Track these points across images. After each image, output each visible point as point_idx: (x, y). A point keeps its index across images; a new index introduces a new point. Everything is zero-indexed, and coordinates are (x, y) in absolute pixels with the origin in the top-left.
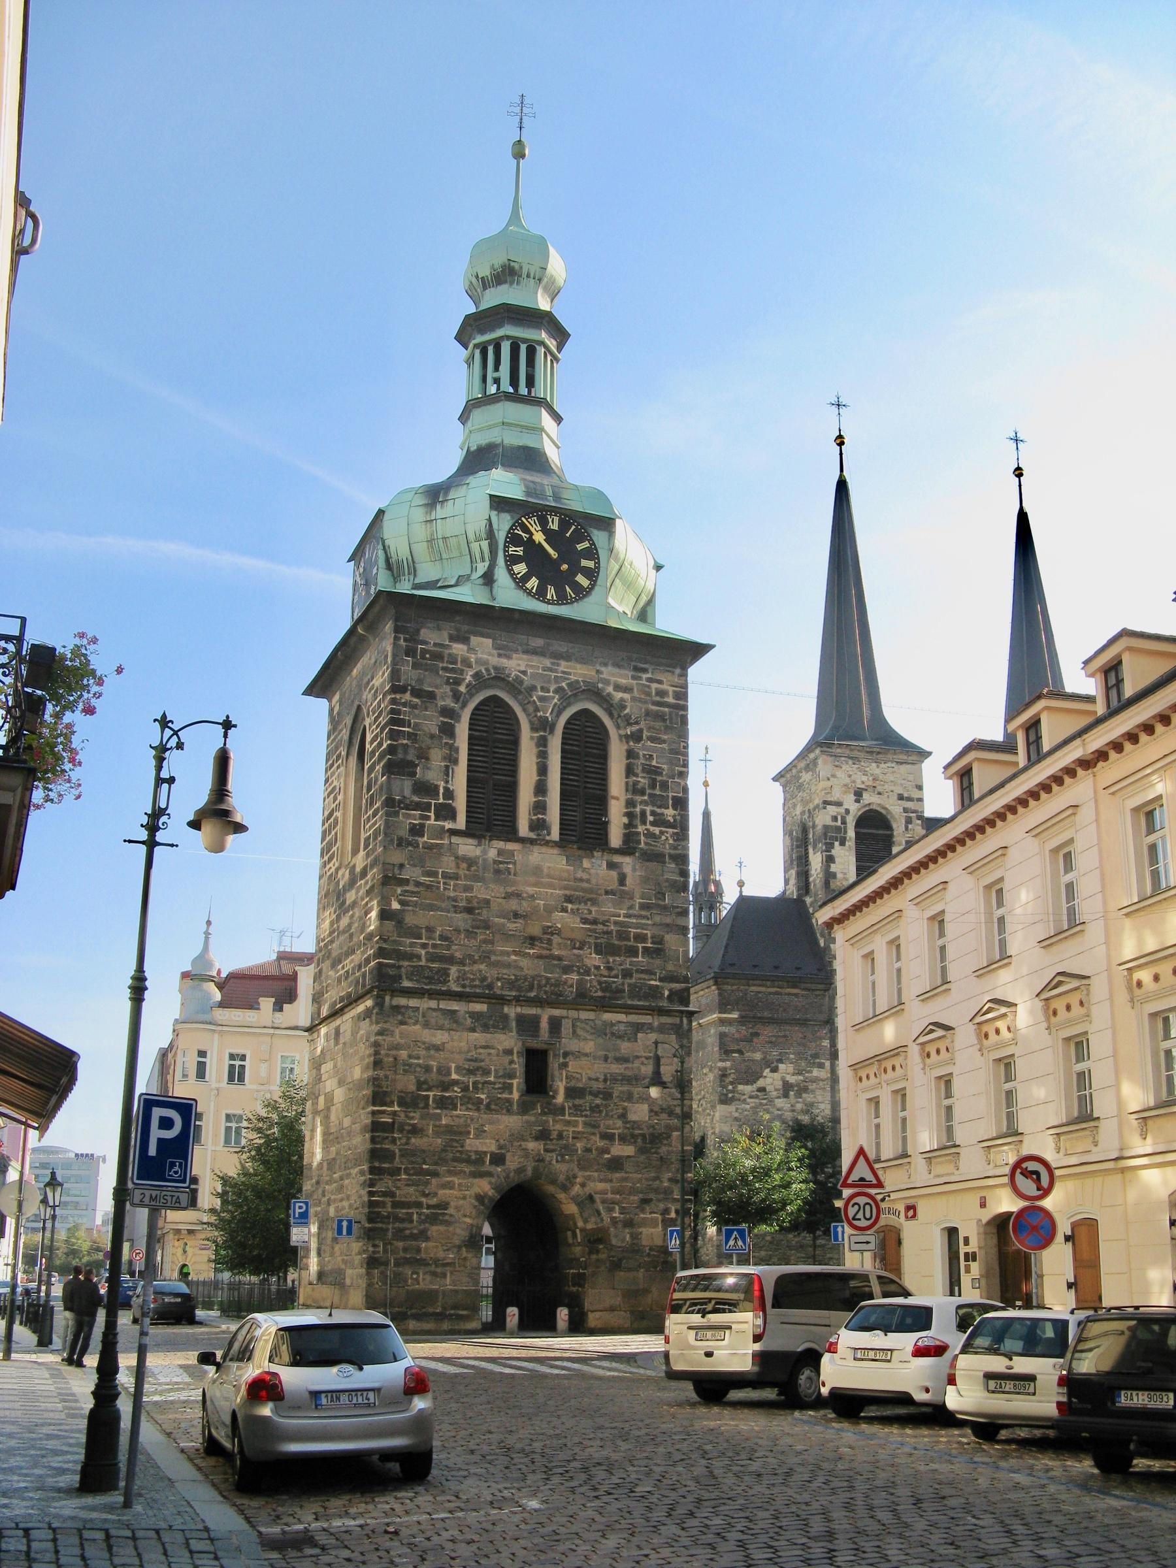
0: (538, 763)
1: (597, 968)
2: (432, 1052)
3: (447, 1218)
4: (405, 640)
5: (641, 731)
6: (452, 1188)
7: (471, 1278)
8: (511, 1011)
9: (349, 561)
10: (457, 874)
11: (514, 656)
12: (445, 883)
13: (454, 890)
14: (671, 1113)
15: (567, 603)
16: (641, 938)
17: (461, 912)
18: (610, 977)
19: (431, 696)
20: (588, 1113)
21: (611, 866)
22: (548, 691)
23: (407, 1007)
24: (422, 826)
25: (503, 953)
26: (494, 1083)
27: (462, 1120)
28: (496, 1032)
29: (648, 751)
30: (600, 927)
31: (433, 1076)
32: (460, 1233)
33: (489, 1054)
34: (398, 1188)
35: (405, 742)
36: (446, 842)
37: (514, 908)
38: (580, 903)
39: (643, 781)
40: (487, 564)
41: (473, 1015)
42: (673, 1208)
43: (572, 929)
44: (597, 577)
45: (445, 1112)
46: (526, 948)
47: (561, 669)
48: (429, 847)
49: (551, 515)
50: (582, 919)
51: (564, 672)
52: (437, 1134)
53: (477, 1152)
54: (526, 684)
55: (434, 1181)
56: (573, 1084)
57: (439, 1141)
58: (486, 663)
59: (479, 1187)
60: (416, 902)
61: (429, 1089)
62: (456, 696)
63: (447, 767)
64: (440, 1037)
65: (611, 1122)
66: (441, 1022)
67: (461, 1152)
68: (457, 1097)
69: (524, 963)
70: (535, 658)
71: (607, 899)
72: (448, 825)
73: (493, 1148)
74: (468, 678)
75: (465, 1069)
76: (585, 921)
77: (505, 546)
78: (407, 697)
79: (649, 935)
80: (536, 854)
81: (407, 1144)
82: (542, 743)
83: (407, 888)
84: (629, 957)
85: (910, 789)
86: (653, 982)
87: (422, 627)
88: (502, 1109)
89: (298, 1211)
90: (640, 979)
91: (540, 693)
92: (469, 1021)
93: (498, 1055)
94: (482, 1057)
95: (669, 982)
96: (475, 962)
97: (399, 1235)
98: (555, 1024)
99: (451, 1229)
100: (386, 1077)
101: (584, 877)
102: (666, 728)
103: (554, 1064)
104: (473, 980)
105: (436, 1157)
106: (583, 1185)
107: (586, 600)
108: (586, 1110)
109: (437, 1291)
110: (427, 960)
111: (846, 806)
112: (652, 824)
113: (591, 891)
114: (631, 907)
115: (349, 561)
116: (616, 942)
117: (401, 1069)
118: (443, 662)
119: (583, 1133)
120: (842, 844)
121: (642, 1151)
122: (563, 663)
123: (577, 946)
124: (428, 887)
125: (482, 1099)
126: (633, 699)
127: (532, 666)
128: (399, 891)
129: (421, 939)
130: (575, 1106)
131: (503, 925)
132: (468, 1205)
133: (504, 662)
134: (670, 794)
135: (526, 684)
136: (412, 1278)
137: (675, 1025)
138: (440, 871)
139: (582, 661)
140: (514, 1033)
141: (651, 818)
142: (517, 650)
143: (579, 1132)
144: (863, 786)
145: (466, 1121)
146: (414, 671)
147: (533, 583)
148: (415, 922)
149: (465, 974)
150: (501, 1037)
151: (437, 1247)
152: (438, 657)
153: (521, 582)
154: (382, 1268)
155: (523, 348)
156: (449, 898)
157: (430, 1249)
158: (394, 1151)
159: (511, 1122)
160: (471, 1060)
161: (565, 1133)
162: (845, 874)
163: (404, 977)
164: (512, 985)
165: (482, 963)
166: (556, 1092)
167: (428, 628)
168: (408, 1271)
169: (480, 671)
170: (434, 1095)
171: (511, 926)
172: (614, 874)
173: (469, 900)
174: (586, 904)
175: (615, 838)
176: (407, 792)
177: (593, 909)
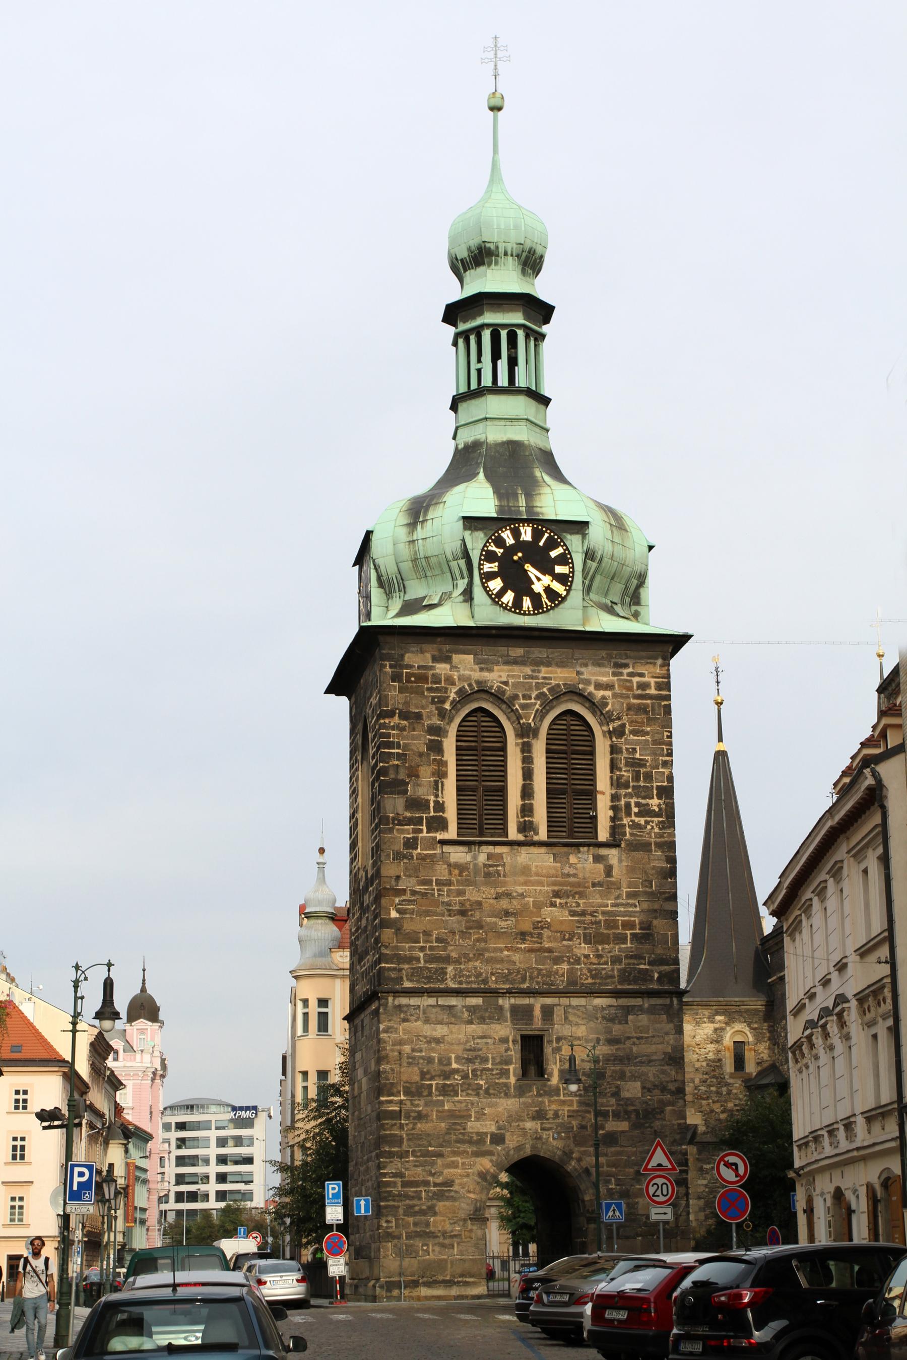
0: (523, 768)
1: (587, 956)
2: (433, 1045)
3: (452, 1194)
4: (391, 666)
5: (623, 726)
6: (457, 1167)
7: (477, 1248)
8: (505, 1003)
9: (354, 565)
10: (450, 880)
11: (496, 668)
12: (438, 890)
13: (448, 896)
14: (664, 1089)
15: (543, 612)
16: (631, 925)
18: (599, 964)
19: (418, 716)
21: (597, 859)
22: (530, 698)
23: (408, 1006)
24: (415, 839)
25: (496, 950)
26: (492, 1070)
27: (464, 1104)
28: (492, 1023)
29: (631, 745)
30: (589, 918)
31: (435, 1067)
32: (464, 1207)
33: (487, 1043)
34: (407, 1169)
35: (396, 762)
36: (438, 851)
37: (504, 907)
38: (568, 897)
39: (626, 774)
40: (466, 581)
43: (562, 922)
44: (572, 582)
45: (447, 1098)
46: (517, 942)
49: (524, 526)
50: (570, 911)
51: (544, 678)
52: (440, 1118)
53: (478, 1134)
54: (508, 694)
55: (439, 1161)
57: (443, 1125)
58: (469, 678)
59: (481, 1165)
60: (413, 909)
61: (432, 1079)
62: (442, 714)
63: (436, 782)
64: (440, 1031)
65: (605, 1100)
66: (440, 1017)
67: (463, 1134)
68: (458, 1084)
69: (516, 957)
70: (515, 668)
72: (440, 836)
73: (493, 1129)
74: (452, 696)
75: (464, 1058)
76: (573, 913)
77: (480, 564)
78: (396, 719)
79: (637, 922)
80: (523, 855)
81: (413, 1129)
82: (526, 749)
83: (404, 898)
84: (617, 944)
86: (642, 967)
87: (406, 652)
88: (501, 1093)
89: (331, 1192)
90: (629, 964)
91: (522, 701)
92: (466, 1014)
93: (494, 1044)
94: (479, 1046)
95: (658, 966)
96: (470, 960)
97: (409, 1211)
98: (548, 1012)
99: (457, 1204)
100: (392, 1070)
101: (571, 873)
102: (649, 719)
103: (548, 1050)
104: (469, 976)
105: (441, 1140)
106: (579, 1160)
107: (561, 606)
109: (446, 1261)
110: (426, 962)
112: (637, 815)
113: (579, 885)
115: (354, 565)
116: (605, 931)
117: (405, 1061)
118: (428, 683)
119: (578, 1111)
121: (635, 1126)
122: (543, 669)
123: (566, 937)
124: (424, 895)
125: (482, 1085)
126: (615, 696)
127: (513, 676)
128: (397, 900)
129: (420, 943)
131: (496, 923)
132: (471, 1182)
133: (486, 675)
134: (655, 785)
135: (508, 694)
136: (423, 1250)
137: (665, 1005)
138: (434, 879)
139: (562, 664)
140: (509, 1023)
141: (636, 810)
142: (499, 663)
143: (573, 1111)
145: (467, 1106)
146: (401, 695)
147: (509, 597)
149: (461, 971)
151: (444, 1221)
152: (423, 678)
153: (496, 598)
154: (396, 1241)
155: (504, 334)
156: (443, 903)
157: (437, 1223)
158: (401, 1137)
159: (508, 1105)
160: (470, 1050)
161: (560, 1113)
163: (405, 979)
164: (505, 978)
165: (476, 961)
166: (551, 1075)
167: (413, 652)
168: (418, 1243)
169: (464, 687)
170: (437, 1084)
171: (503, 924)
172: (600, 867)
173: (462, 904)
174: (574, 897)
175: (603, 835)
176: (400, 808)
177: (581, 902)
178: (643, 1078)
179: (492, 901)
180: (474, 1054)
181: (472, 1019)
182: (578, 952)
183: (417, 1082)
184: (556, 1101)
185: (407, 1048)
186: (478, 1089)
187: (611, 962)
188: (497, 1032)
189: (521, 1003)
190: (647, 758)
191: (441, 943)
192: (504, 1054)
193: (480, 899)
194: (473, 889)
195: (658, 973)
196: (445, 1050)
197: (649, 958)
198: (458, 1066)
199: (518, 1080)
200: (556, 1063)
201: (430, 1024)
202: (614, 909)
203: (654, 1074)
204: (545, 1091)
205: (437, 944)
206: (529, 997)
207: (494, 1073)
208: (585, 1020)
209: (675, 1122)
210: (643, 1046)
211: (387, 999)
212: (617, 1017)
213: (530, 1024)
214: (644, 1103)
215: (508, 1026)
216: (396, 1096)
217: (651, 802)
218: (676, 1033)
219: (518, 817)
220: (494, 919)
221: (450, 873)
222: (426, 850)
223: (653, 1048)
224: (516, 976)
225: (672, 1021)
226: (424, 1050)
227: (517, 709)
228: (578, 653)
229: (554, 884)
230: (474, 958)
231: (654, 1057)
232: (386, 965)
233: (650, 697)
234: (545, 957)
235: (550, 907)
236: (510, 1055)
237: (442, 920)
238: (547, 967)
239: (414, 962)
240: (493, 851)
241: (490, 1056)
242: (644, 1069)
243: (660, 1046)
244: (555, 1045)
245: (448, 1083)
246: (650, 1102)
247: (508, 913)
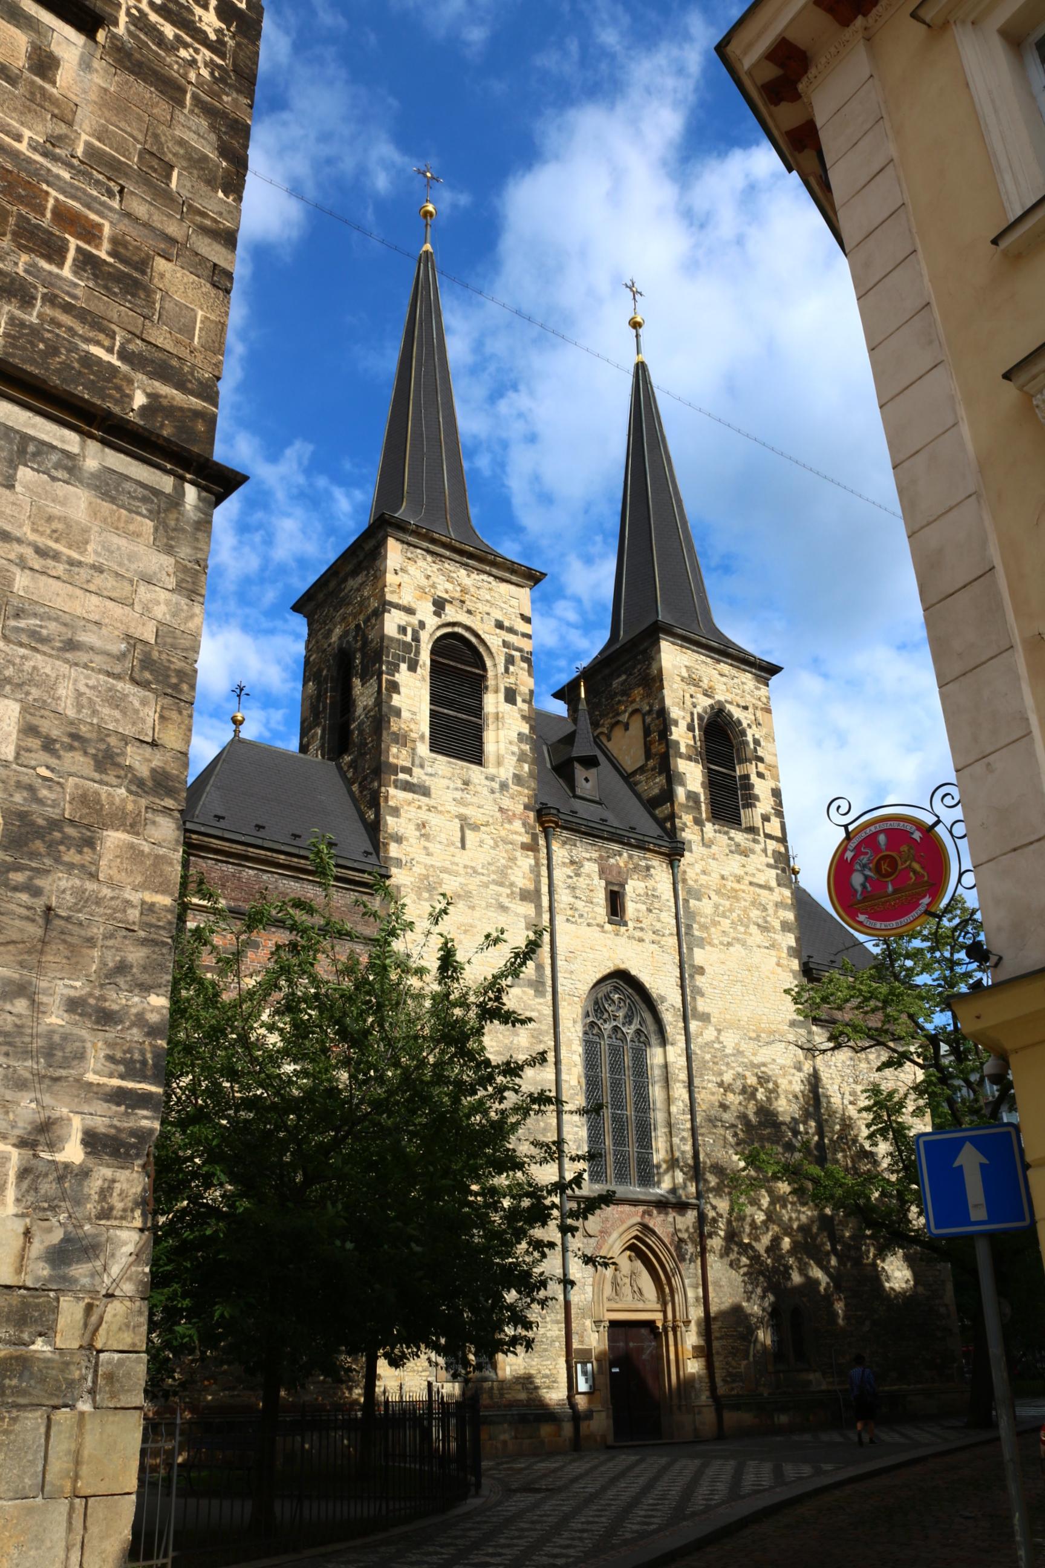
42: (77, 1124)
79: (107, 230)
84: (29, 250)
85: (513, 617)
90: (53, 321)
111: (419, 616)
114: (54, 140)
120: (413, 667)
137: (157, 492)
144: (446, 596)
162: (414, 713)
178: (35, 692)
202: (37, 157)
203: (79, 694)
209: (135, 897)
214: (19, 785)
217: (198, 11)
218: (179, 589)
223: (90, 606)
225: (169, 550)
231: (87, 638)
242: (44, 664)
243: (117, 610)
246: (44, 793)
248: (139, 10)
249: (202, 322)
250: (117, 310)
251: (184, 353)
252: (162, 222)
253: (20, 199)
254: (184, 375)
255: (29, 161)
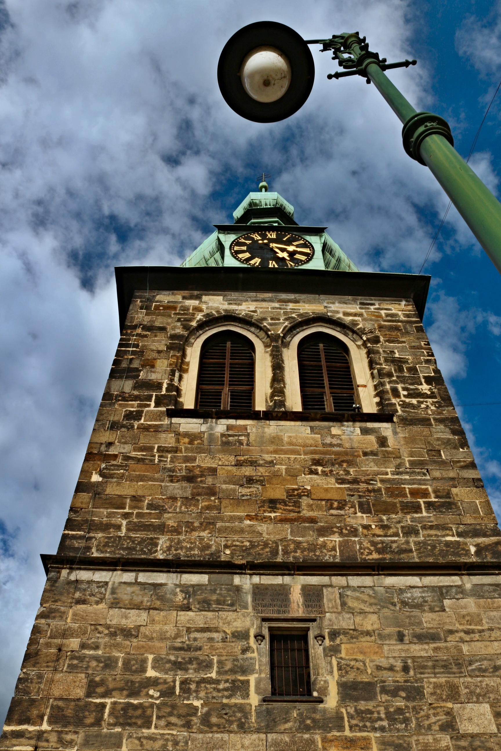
1: (367, 527)
2: (119, 639)
4: (141, 302)
12: (159, 456)
13: (172, 461)
17: (178, 481)
18: (386, 536)
20: (385, 723)
21: (365, 431)
25: (232, 519)
26: (218, 682)
30: (363, 486)
33: (211, 639)
37: (247, 474)
41: (187, 590)
43: (327, 490)
46: (264, 511)
47: (289, 307)
48: (146, 428)
51: (292, 309)
56: (351, 677)
60: (123, 474)
61: (106, 694)
62: (186, 327)
65: (430, 738)
66: (137, 599)
68: (152, 705)
69: (263, 528)
71: (367, 460)
75: (169, 661)
76: (342, 481)
79: (430, 489)
80: (272, 428)
84: (408, 513)
87: (158, 295)
88: (231, 723)
90: (429, 536)
91: (270, 321)
92: (180, 597)
93: (224, 640)
94: (198, 644)
96: (194, 529)
100: (40, 676)
104: (191, 549)
108: (381, 719)
110: (128, 530)
113: (346, 453)
114: (398, 466)
124: (139, 460)
125: (196, 709)
130: (359, 712)
131: (234, 490)
141: (405, 393)
148: (117, 493)
149: (179, 542)
150: (231, 616)
156: (164, 469)
160: (181, 649)
165: (204, 530)
166: (324, 691)
167: (164, 294)
171: (244, 491)
172: (372, 438)
174: (340, 465)
179: (230, 468)
180: (188, 655)
181: (189, 603)
182: (350, 521)
183: (79, 700)
184: (337, 738)
185: (74, 643)
186: (188, 715)
187: (404, 534)
188: (229, 623)
189: (270, 582)
190: (407, 357)
191: (155, 510)
192: (240, 657)
193: (214, 466)
194: (206, 457)
195: (475, 546)
196: (138, 648)
197: (458, 528)
198: (158, 675)
199: (264, 700)
200: (331, 672)
201: (120, 608)
202: (396, 477)
204: (314, 720)
205: (148, 511)
206: (283, 575)
207: (221, 687)
208: (374, 607)
210: (479, 644)
211: (59, 572)
212: (426, 602)
213: (284, 612)
215: (248, 614)
216: (34, 724)
217: (420, 387)
219: (267, 401)
220: (232, 486)
221: (178, 441)
222: (151, 421)
224: (262, 549)
226: (102, 646)
227: (265, 326)
228: (322, 297)
229: (312, 453)
230: (200, 527)
232: (70, 533)
233: (401, 321)
234: (305, 527)
235: (309, 474)
236: (251, 658)
237: (161, 486)
238: (310, 539)
239: (111, 530)
240: (235, 423)
241: (215, 659)
244: (327, 642)
245: (136, 702)
247: (253, 480)
248: (402, 401)
249: (480, 504)
250: (448, 518)
251: (479, 521)
252: (447, 474)
253: (397, 496)
254: (484, 530)
255: (394, 480)
